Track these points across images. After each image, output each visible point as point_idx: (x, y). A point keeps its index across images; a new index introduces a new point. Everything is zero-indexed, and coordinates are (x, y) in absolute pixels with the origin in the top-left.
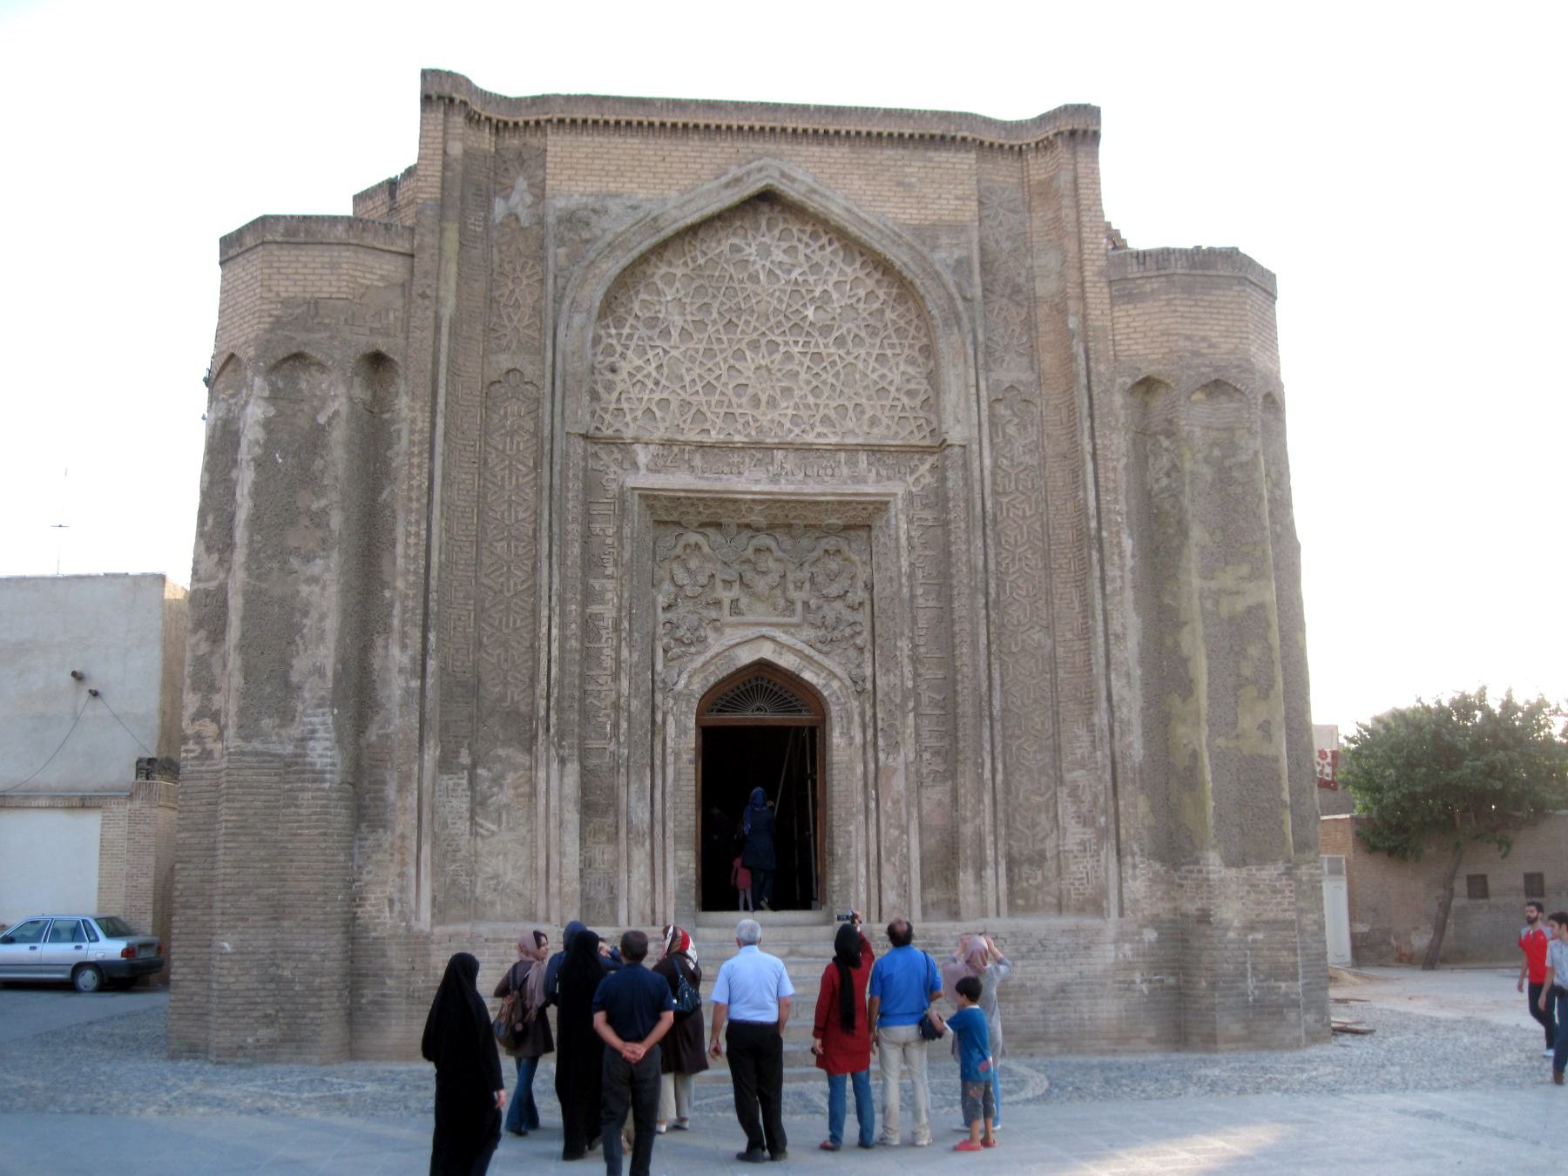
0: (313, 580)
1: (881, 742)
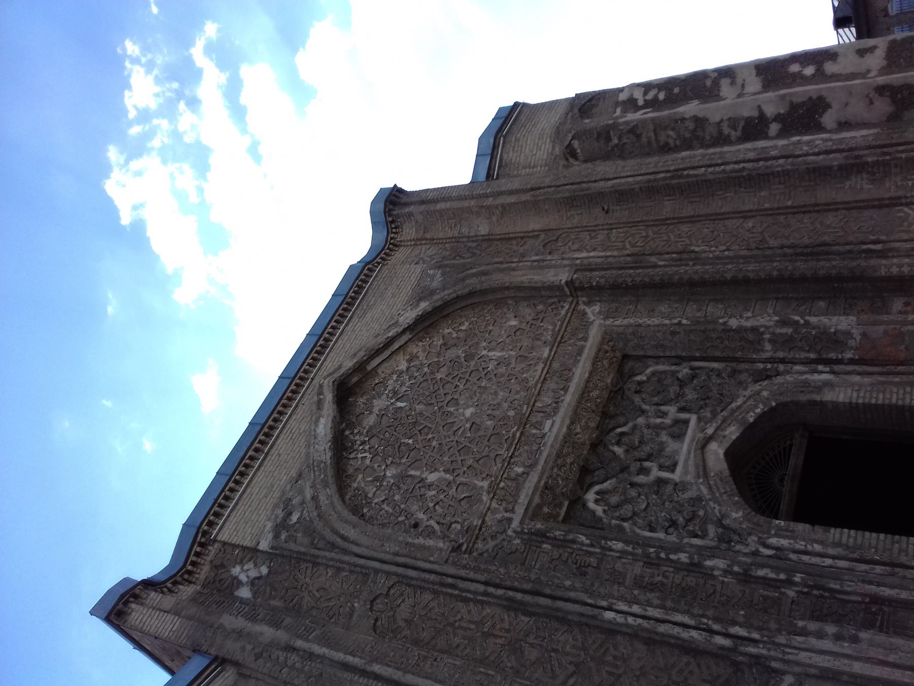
1: (832, 355)
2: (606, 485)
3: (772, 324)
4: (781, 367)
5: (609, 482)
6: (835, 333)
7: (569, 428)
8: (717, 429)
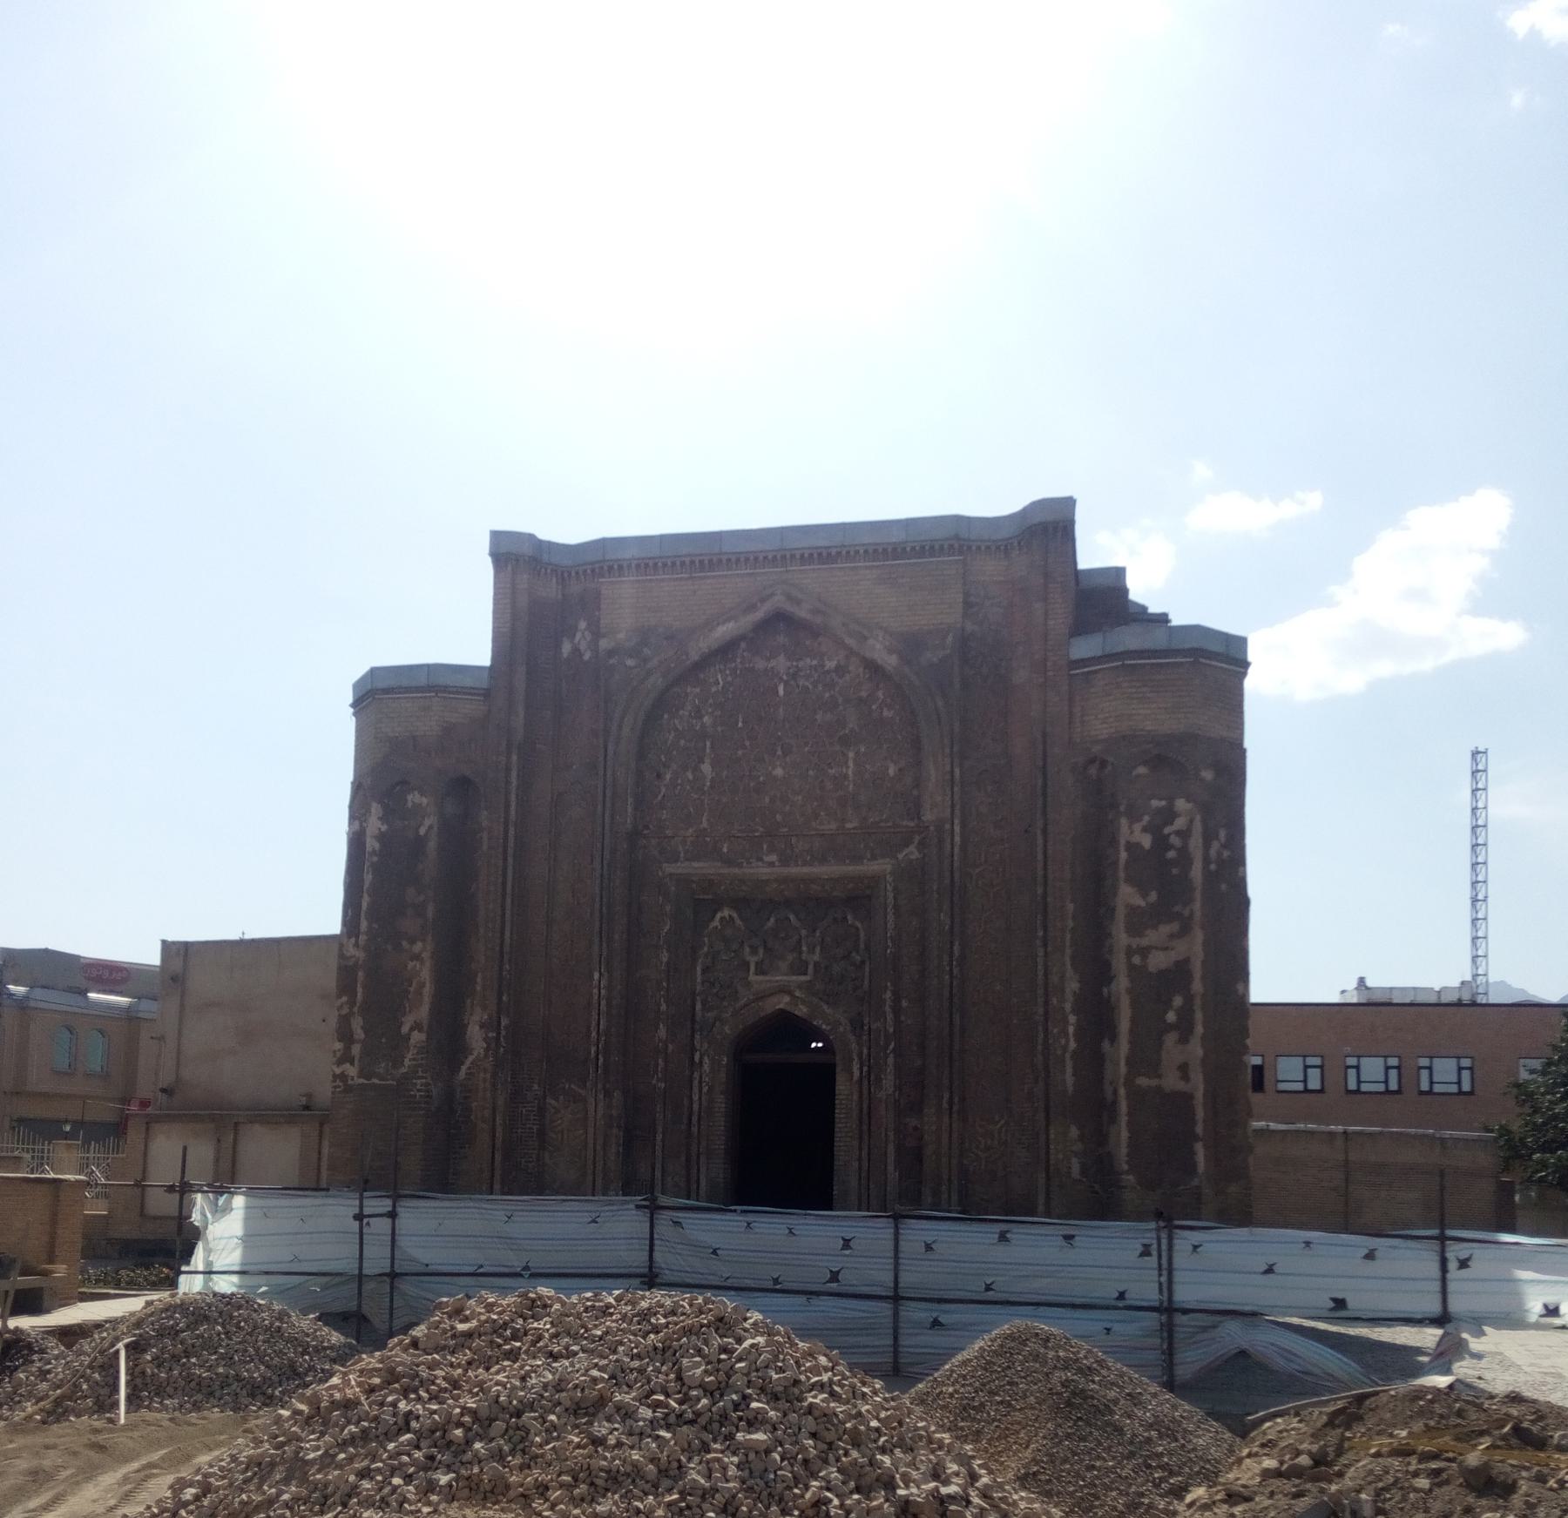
0: (417, 957)
2: (738, 922)
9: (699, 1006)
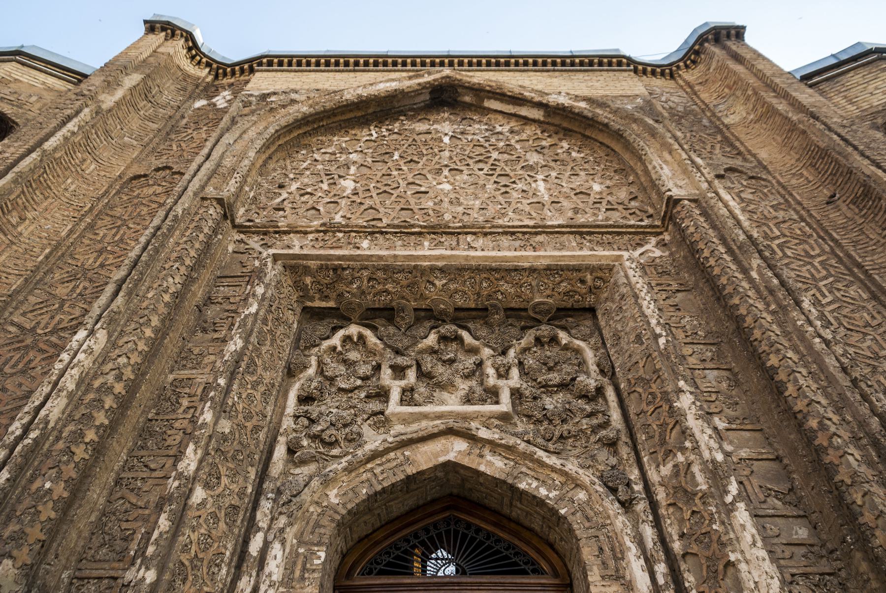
3: (706, 455)
4: (641, 506)
5: (378, 342)
6: (729, 564)
7: (433, 269)
8: (490, 442)
9: (280, 451)
